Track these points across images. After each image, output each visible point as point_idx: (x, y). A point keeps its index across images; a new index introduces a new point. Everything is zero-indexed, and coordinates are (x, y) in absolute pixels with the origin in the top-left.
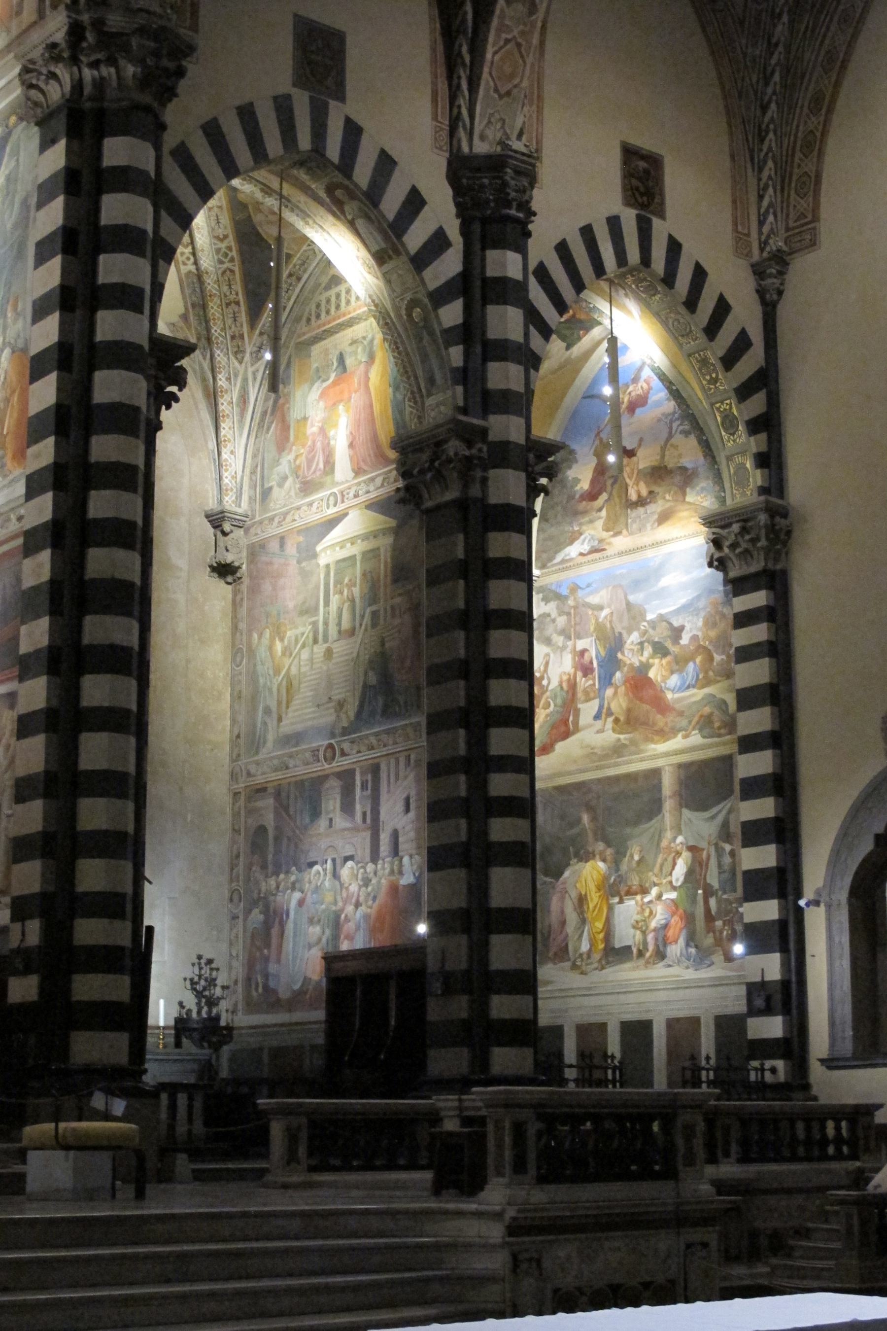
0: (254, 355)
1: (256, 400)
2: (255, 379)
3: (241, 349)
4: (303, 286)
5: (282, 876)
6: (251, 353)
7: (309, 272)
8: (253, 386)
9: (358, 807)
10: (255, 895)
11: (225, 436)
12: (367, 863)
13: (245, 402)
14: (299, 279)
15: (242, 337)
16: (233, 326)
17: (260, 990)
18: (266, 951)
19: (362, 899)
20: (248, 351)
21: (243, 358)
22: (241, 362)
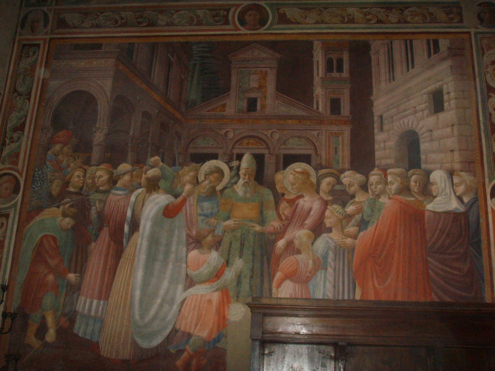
5: (124, 167)
9: (318, 91)
10: (55, 189)
12: (342, 171)
17: (51, 336)
18: (72, 276)
19: (328, 222)
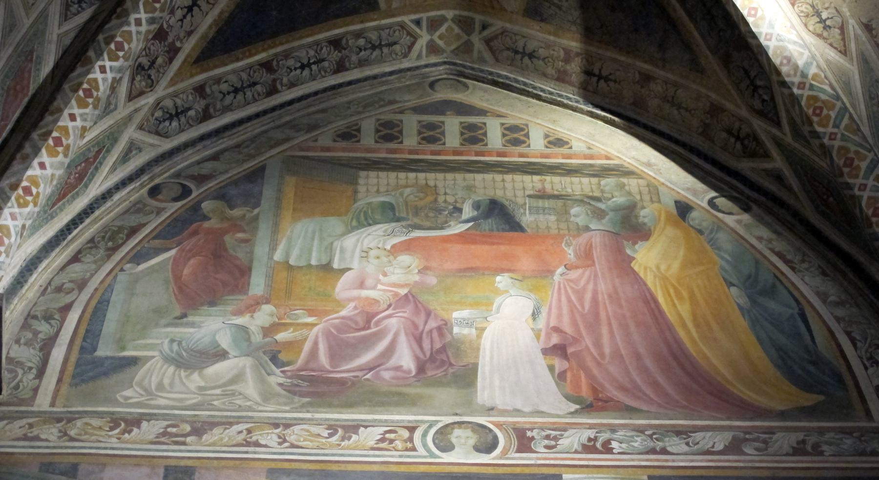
0: (158, 114)
1: (106, 196)
2: (125, 158)
3: (152, 72)
4: (341, 85)
6: (157, 104)
7: (368, 72)
8: (113, 169)
11: (34, 181)
13: (80, 178)
14: (340, 67)
15: (173, 52)
16: (179, 13)
20: (160, 91)
21: (141, 93)
22: (131, 97)
